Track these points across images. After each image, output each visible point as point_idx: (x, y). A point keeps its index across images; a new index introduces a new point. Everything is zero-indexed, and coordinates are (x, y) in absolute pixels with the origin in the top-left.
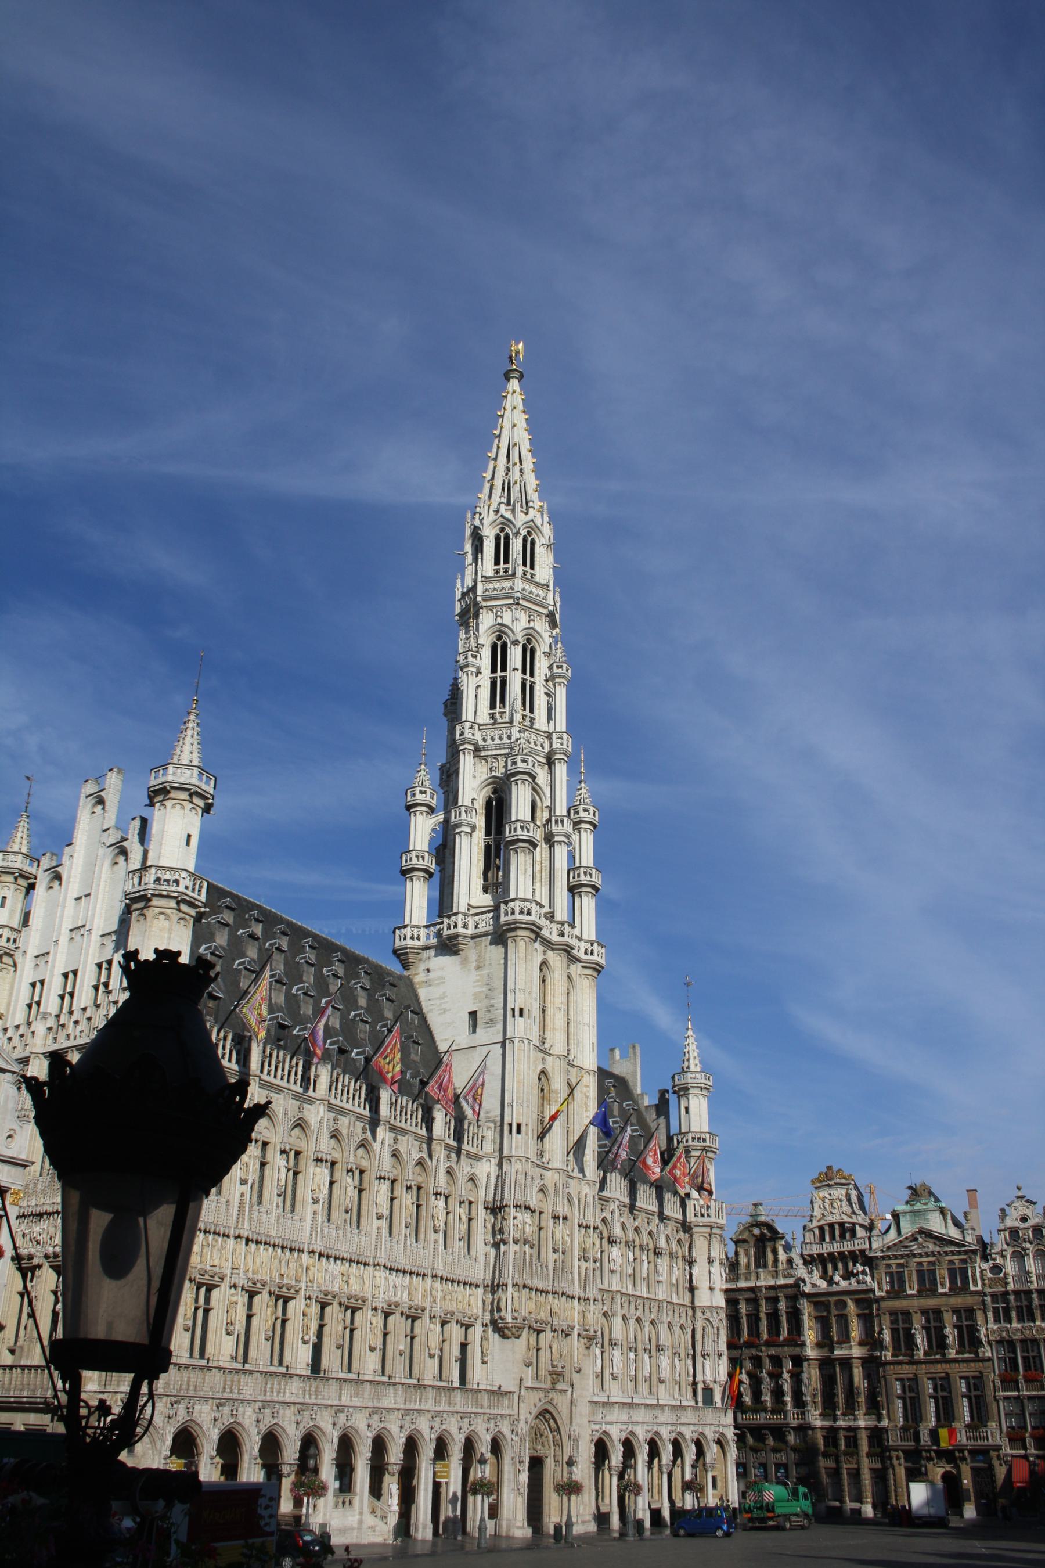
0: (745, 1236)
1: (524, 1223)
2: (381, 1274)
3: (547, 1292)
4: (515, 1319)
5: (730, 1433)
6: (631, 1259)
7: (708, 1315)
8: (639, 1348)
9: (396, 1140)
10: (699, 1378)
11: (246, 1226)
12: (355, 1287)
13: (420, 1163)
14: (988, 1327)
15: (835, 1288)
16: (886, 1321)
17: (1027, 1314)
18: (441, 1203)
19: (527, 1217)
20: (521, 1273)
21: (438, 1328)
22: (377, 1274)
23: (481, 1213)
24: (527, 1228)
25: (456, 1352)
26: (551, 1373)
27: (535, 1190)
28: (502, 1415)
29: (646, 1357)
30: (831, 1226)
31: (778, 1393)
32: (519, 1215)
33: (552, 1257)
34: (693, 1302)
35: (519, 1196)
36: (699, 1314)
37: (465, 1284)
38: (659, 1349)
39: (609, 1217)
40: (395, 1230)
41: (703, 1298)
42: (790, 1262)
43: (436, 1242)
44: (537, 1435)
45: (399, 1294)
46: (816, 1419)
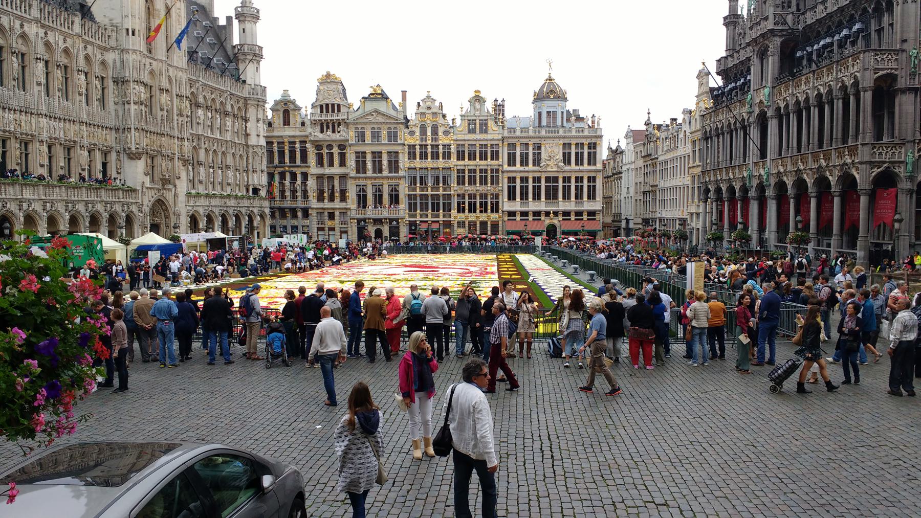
0: (278, 107)
1: (141, 92)
2: (44, 121)
5: (267, 211)
6: (210, 116)
7: (256, 150)
9: (46, 34)
12: (25, 128)
13: (66, 51)
14: (404, 161)
15: (328, 138)
16: (353, 157)
17: (423, 156)
18: (83, 77)
19: (142, 89)
20: (140, 121)
21: (86, 153)
22: (41, 120)
23: (110, 85)
25: (99, 167)
26: (161, 180)
27: (147, 72)
29: (220, 172)
30: (327, 105)
31: (294, 192)
33: (160, 113)
34: (246, 142)
35: (135, 75)
36: (251, 150)
38: (228, 167)
40: (51, 93)
41: (253, 141)
42: (303, 124)
43: (80, 101)
44: (153, 212)
46: (314, 203)
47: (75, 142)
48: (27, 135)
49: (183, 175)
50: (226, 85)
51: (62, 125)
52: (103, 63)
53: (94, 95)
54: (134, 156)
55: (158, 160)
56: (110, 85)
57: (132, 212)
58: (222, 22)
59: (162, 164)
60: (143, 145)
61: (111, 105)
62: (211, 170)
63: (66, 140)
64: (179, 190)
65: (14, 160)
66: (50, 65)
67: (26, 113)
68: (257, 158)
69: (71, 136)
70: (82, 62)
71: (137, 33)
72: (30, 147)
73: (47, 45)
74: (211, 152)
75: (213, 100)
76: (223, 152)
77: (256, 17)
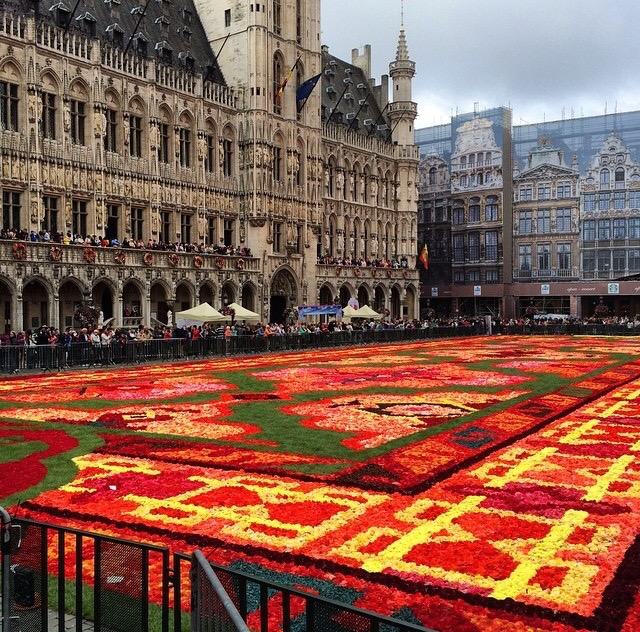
3: (284, 199)
4: (259, 214)
5: (416, 284)
8: (358, 235)
9: (164, 97)
10: (399, 253)
11: (38, 151)
12: (137, 194)
13: (186, 114)
19: (266, 151)
22: (154, 185)
24: (265, 157)
28: (251, 273)
32: (260, 149)
33: (287, 177)
36: (400, 217)
37: (226, 194)
38: (372, 236)
39: (336, 155)
40: (169, 159)
41: (403, 206)
45: (174, 199)
47: (193, 209)
48: (138, 200)
49: (314, 244)
50: (373, 147)
51: (179, 191)
52: (229, 127)
53: (218, 160)
54: (258, 223)
55: (284, 227)
56: (237, 150)
57: (251, 282)
58: (378, 83)
59: (289, 233)
60: (265, 210)
61: (236, 171)
62: (352, 239)
63: (183, 207)
64: (307, 260)
65: (124, 227)
66: (169, 130)
67: (139, 178)
68: (408, 226)
69: (190, 203)
70: (202, 126)
71: (261, 91)
72: (144, 214)
73: (164, 108)
74: (352, 220)
75: (357, 163)
76: (367, 220)
77: (411, 72)
